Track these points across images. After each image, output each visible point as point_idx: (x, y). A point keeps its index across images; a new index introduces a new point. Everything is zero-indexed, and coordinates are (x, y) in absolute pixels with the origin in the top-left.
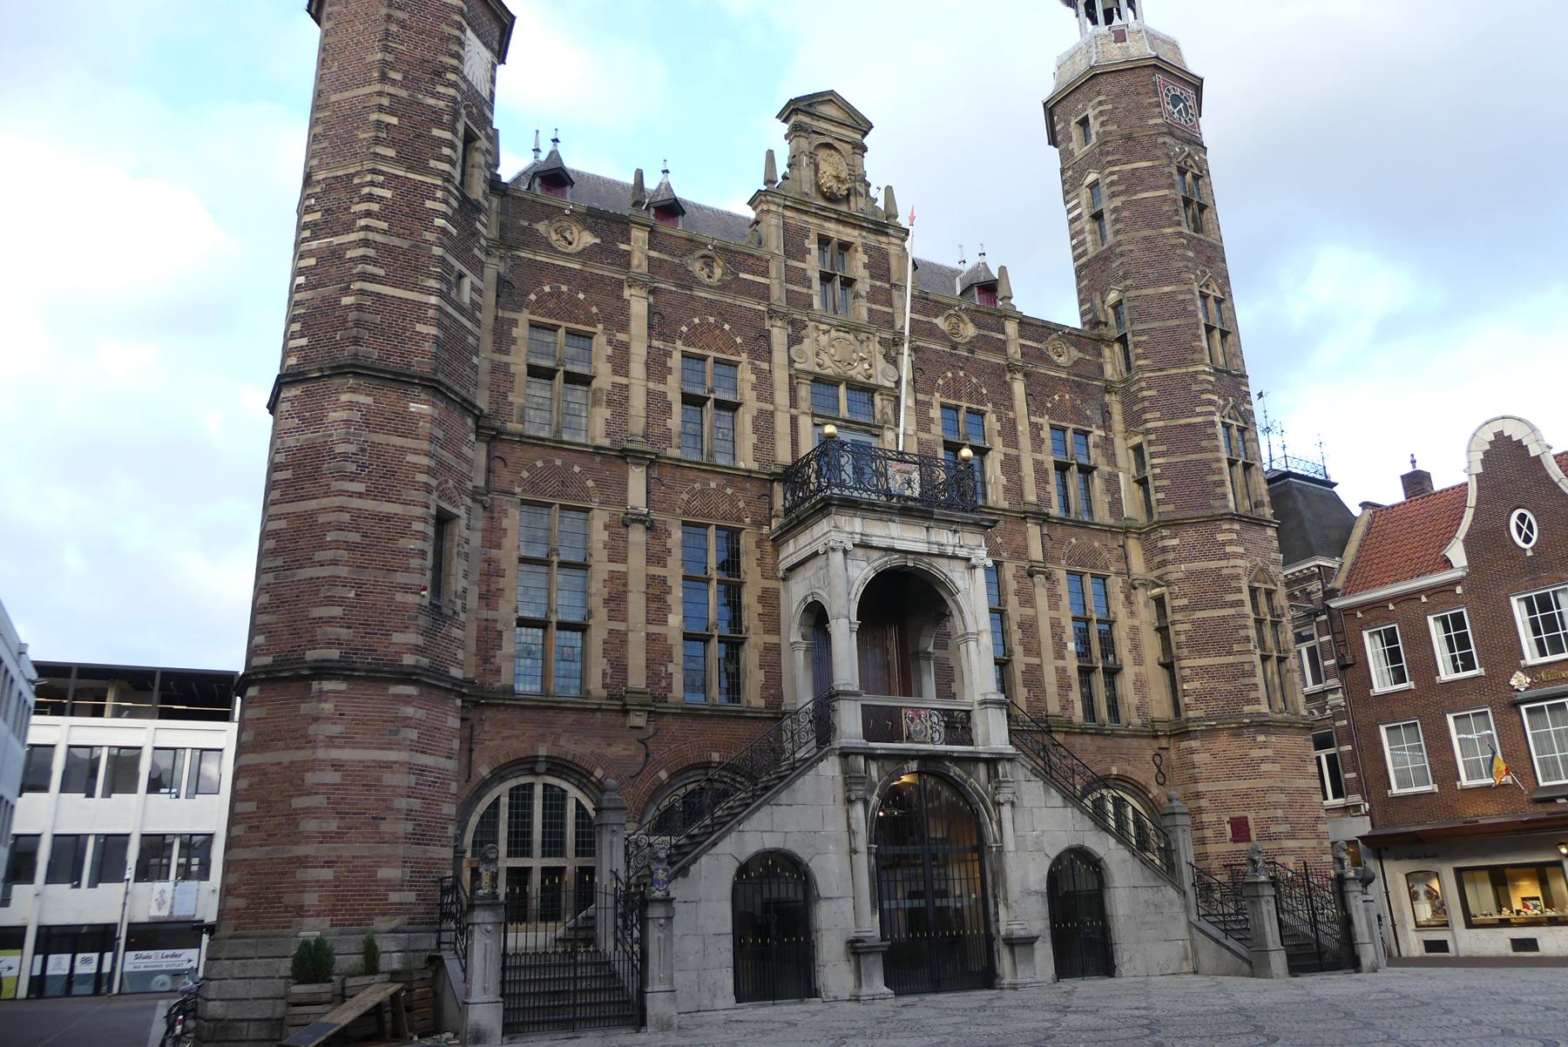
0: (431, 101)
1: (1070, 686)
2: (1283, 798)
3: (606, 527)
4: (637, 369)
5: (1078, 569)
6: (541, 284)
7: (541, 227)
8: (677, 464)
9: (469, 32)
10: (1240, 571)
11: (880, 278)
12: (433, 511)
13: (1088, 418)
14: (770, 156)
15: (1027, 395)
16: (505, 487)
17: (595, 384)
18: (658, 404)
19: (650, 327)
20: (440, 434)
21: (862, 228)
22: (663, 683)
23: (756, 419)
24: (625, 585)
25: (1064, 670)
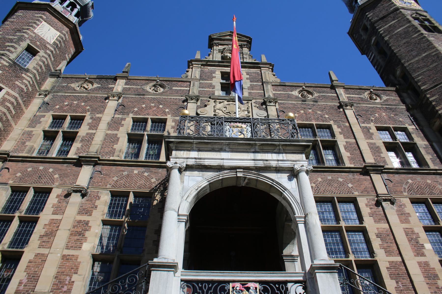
3: (58, 196)
4: (103, 126)
5: (418, 196)
6: (64, 102)
7: (73, 85)
8: (114, 163)
9: (44, 22)
13: (401, 121)
16: (4, 181)
17: (78, 134)
18: (111, 139)
19: (116, 110)
22: (65, 288)
24: (58, 227)
25: (426, 264)
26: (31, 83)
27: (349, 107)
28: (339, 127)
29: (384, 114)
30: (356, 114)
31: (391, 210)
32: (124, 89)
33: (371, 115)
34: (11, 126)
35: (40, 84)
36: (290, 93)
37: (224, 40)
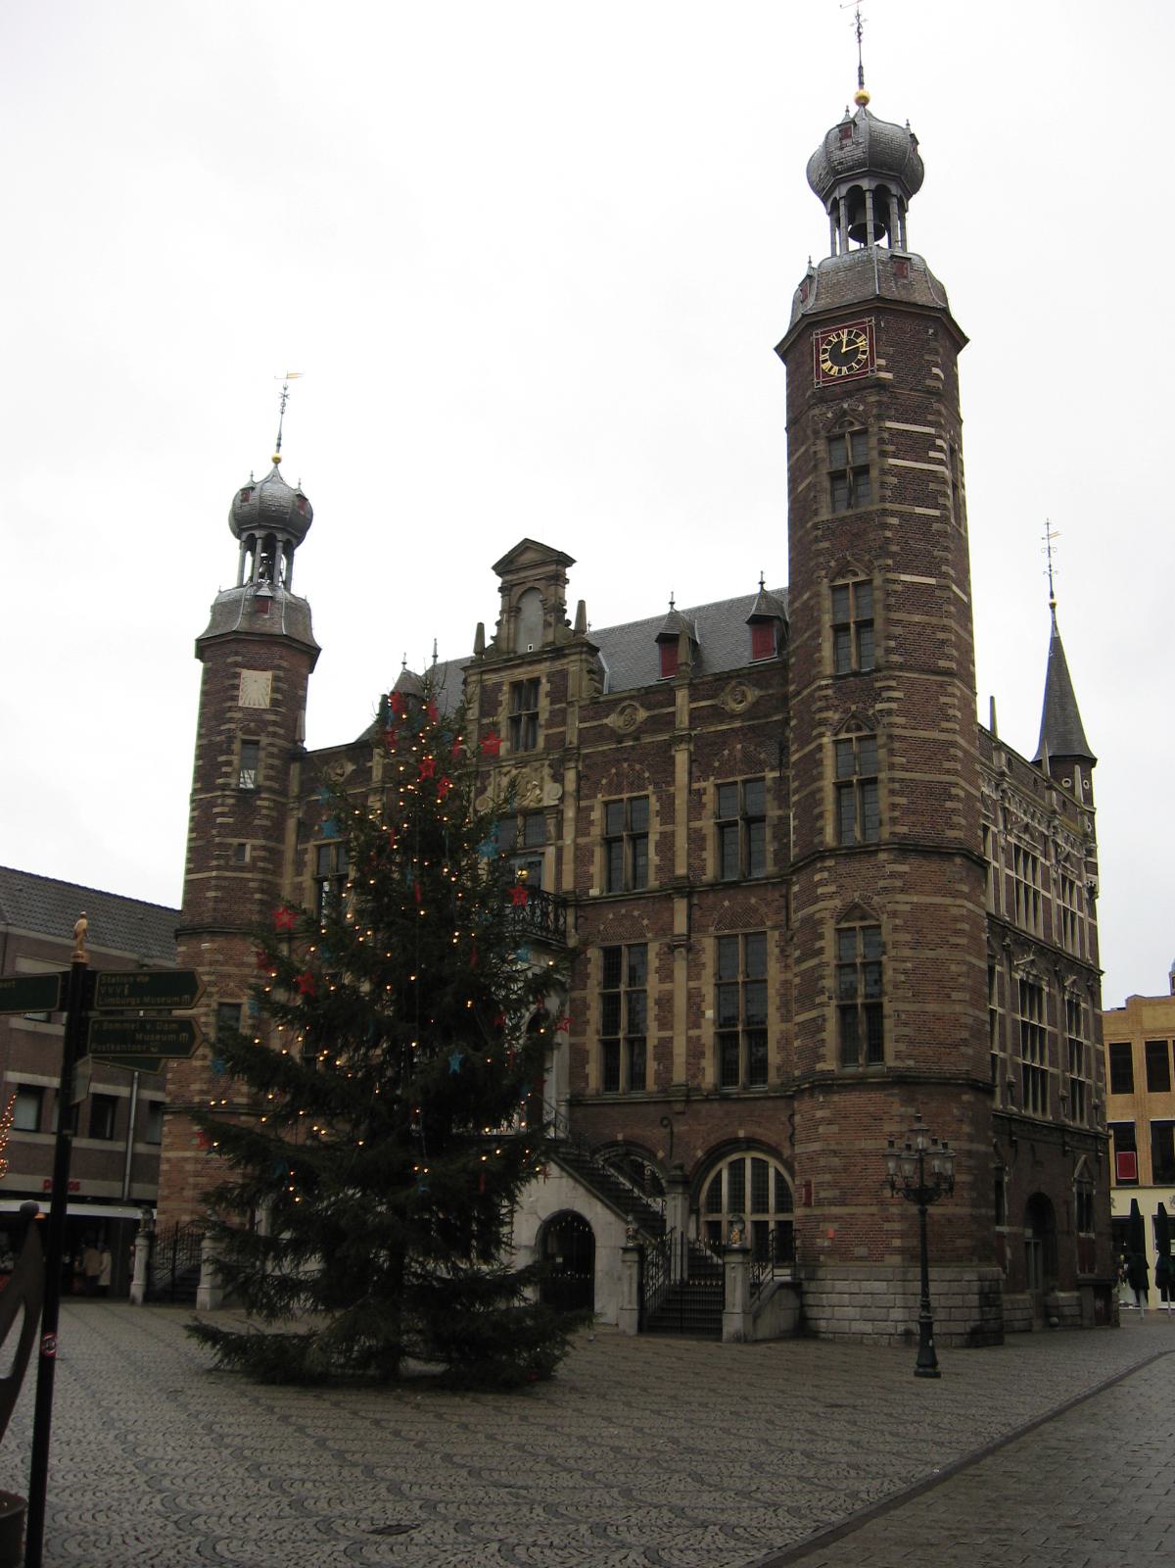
0: (218, 738)
1: (702, 1054)
2: (836, 1161)
9: (246, 673)
10: (824, 914)
11: (560, 702)
12: (215, 1006)
14: (481, 627)
15: (691, 761)
20: (221, 958)
21: (546, 659)
25: (699, 1038)
26: (272, 805)
27: (683, 746)
28: (659, 799)
29: (739, 746)
30: (693, 758)
33: (716, 755)
34: (277, 885)
35: (283, 792)
36: (605, 721)
37: (518, 570)
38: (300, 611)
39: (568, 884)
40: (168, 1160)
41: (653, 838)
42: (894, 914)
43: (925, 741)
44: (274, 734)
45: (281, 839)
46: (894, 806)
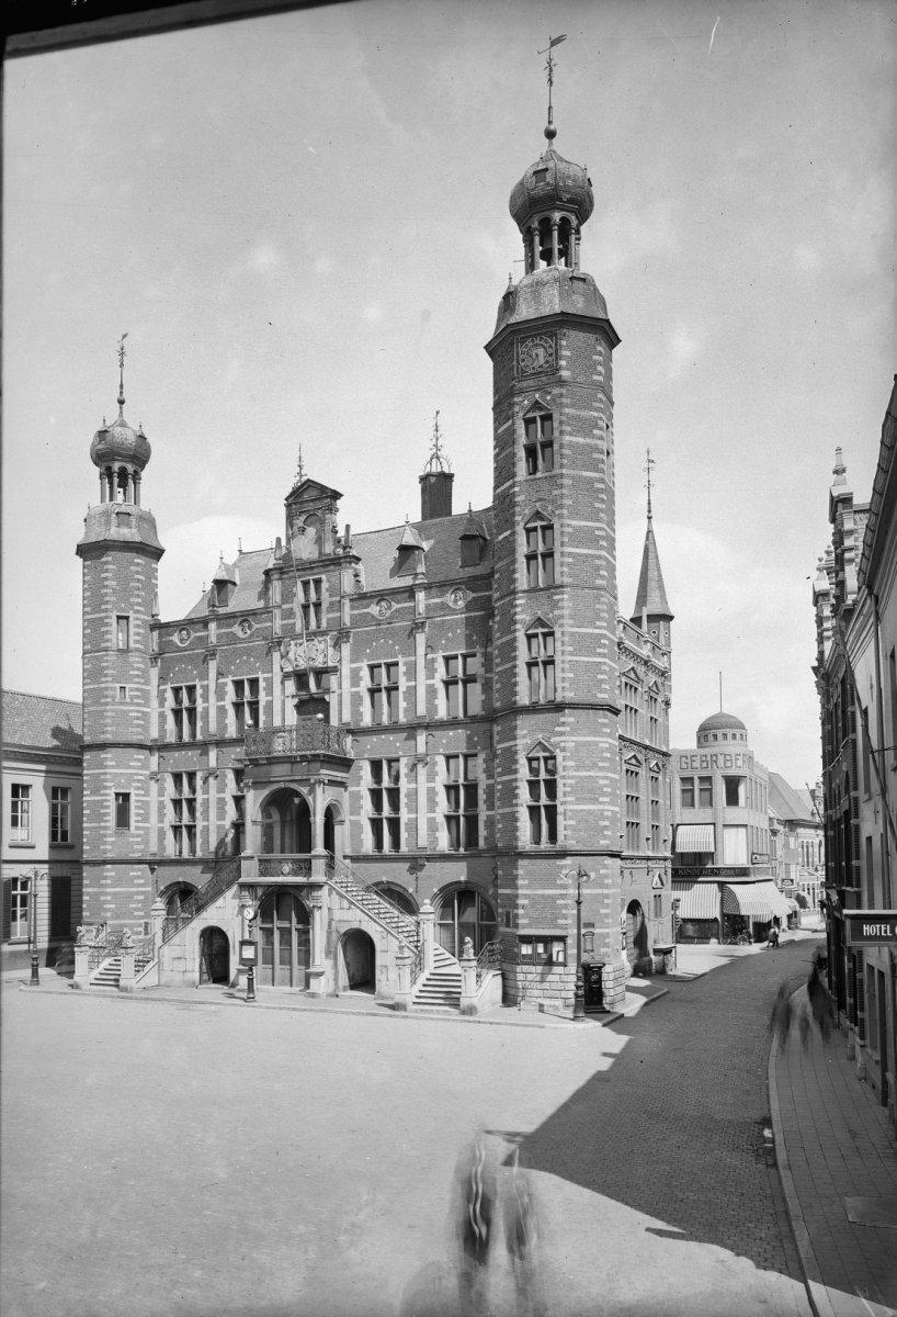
4: (212, 697)
7: (175, 638)
23: (265, 707)
25: (434, 819)
31: (422, 771)
32: (219, 637)
38: (148, 521)
39: (347, 717)
40: (88, 894)
41: (402, 689)
42: (563, 750)
43: (585, 634)
44: (138, 611)
45: (147, 683)
46: (563, 679)
